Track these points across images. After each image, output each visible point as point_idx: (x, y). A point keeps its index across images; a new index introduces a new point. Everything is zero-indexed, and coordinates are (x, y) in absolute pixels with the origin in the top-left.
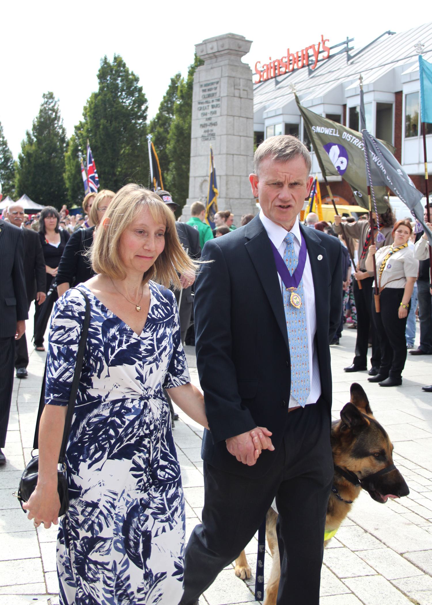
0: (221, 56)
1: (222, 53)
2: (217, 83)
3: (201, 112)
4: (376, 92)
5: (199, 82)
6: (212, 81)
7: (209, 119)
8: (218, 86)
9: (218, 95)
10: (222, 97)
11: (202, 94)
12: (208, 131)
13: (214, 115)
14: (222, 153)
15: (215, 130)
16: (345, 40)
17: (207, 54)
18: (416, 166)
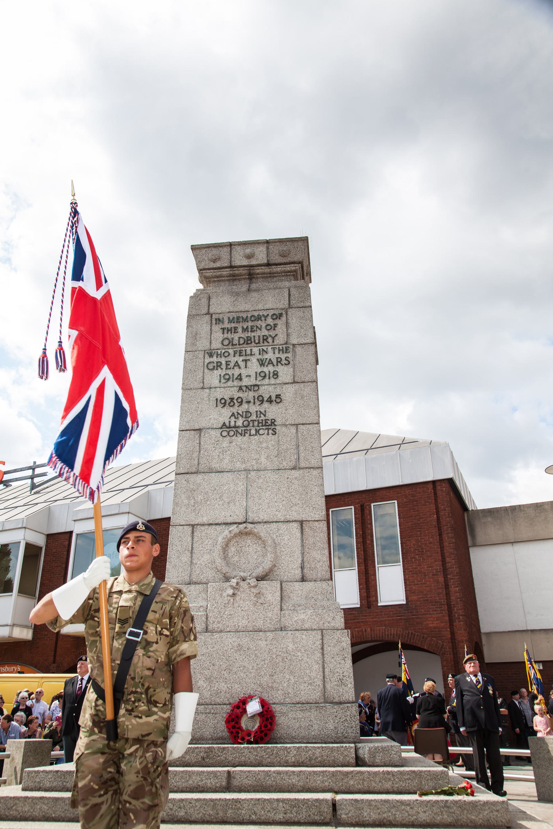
0: (271, 275)
1: (279, 269)
4: (130, 514)
5: (208, 313)
6: (256, 314)
7: (249, 388)
8: (281, 323)
9: (281, 339)
10: (294, 345)
11: (218, 336)
13: (273, 381)
14: (302, 465)
15: (272, 411)
16: (32, 464)
17: (231, 267)
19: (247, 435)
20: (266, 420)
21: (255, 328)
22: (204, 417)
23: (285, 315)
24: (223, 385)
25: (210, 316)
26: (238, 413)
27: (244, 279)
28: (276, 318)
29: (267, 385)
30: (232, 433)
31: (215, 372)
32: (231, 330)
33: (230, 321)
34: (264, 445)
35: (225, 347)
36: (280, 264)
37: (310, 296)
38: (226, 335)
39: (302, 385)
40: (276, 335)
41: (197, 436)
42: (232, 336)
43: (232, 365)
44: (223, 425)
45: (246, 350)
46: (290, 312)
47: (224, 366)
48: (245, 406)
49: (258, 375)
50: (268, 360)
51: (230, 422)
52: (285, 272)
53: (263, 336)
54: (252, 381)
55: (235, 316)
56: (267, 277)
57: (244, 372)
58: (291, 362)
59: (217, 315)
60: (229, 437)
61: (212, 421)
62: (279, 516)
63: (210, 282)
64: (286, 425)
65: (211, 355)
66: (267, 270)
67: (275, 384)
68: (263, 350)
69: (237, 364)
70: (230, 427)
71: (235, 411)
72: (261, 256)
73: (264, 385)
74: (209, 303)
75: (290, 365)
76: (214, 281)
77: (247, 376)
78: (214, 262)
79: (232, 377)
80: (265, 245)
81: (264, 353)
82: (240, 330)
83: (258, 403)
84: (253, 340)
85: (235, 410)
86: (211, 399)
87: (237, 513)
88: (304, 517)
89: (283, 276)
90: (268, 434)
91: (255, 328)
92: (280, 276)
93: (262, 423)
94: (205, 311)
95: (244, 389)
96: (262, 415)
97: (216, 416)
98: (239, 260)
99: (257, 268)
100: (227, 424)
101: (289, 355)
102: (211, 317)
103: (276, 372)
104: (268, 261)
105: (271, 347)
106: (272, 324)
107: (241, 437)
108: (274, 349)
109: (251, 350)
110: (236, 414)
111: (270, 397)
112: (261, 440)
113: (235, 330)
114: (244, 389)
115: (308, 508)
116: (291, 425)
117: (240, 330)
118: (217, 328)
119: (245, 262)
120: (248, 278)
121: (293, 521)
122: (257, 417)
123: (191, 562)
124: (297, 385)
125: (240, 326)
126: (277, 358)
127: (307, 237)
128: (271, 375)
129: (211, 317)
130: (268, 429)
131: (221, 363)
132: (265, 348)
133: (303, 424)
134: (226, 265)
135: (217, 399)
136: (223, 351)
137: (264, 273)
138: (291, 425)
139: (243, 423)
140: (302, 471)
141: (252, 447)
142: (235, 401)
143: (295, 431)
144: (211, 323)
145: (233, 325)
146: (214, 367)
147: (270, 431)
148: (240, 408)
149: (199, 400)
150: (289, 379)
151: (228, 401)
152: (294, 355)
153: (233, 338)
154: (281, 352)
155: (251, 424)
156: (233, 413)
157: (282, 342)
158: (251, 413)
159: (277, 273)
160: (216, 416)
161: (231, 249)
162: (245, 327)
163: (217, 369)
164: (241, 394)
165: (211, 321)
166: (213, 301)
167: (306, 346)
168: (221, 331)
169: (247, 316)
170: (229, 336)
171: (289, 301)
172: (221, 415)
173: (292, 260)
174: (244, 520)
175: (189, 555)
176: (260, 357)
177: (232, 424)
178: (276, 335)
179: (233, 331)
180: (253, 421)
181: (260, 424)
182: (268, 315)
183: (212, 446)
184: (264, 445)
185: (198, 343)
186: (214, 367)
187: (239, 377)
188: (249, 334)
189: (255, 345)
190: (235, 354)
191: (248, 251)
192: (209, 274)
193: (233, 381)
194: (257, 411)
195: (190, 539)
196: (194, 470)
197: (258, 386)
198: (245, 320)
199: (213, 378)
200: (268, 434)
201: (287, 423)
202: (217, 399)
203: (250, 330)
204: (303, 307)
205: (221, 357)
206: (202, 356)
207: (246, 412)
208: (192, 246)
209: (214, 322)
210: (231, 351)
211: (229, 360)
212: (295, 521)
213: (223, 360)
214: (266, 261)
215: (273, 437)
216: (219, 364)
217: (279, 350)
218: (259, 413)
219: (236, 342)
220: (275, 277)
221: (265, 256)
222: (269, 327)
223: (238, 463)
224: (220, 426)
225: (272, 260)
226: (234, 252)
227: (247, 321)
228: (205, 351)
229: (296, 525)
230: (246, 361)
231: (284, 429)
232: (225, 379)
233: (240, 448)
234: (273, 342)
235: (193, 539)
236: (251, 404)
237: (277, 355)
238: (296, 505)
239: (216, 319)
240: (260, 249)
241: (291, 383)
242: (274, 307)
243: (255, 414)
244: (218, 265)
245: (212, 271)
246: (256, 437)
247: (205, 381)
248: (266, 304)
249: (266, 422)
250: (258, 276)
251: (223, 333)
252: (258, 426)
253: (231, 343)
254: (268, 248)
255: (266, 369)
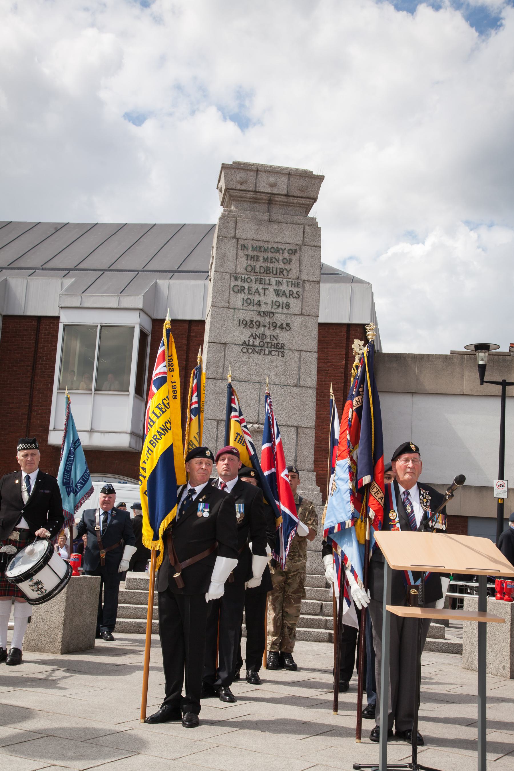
0: (288, 204)
1: (296, 200)
2: (295, 252)
3: (241, 296)
5: (234, 237)
6: (275, 246)
8: (295, 258)
9: (294, 274)
10: (304, 281)
11: (243, 262)
12: (263, 336)
13: (285, 311)
14: (302, 383)
15: (283, 337)
17: (255, 191)
18: (87, 434)
19: (262, 354)
20: (277, 343)
21: (274, 260)
22: (229, 333)
23: (298, 252)
24: (245, 308)
25: (236, 240)
26: (256, 335)
27: (264, 203)
28: (291, 254)
29: (280, 313)
30: (250, 351)
31: (239, 295)
32: (254, 258)
33: (254, 250)
34: (274, 364)
35: (248, 273)
36: (297, 197)
37: (320, 237)
38: (249, 262)
39: (307, 318)
40: (291, 269)
41: (222, 349)
42: (255, 264)
43: (253, 290)
44: (244, 343)
45: (265, 279)
46: (304, 249)
47: (246, 291)
48: (262, 329)
49: (274, 303)
50: (283, 291)
51: (249, 341)
52: (300, 204)
53: (280, 268)
54: (268, 308)
55: (258, 245)
56: (283, 205)
57: (262, 298)
58: (301, 296)
59: (243, 241)
60: (248, 354)
61: (235, 338)
62: (282, 421)
63: (233, 200)
64: (292, 350)
65: (236, 279)
66: (285, 199)
67: (286, 314)
68: (279, 281)
69: (257, 291)
70: (249, 345)
71: (254, 332)
72: (282, 187)
73: (278, 313)
74: (236, 227)
75: (300, 299)
76: (238, 200)
77: (265, 303)
78: (241, 184)
79: (252, 301)
80: (287, 176)
81: (280, 284)
82: (261, 259)
83: (272, 328)
84: (271, 271)
85: (254, 331)
86: (235, 318)
87: (251, 415)
88: (299, 424)
89: (297, 207)
90: (278, 356)
91: (274, 260)
92: (295, 206)
93: (274, 345)
94: (232, 235)
95: (262, 314)
96: (274, 339)
97: (238, 335)
98: (263, 187)
99: (277, 196)
100: (247, 343)
101: (300, 290)
102: (238, 241)
103: (288, 304)
104: (288, 192)
105: (285, 280)
106: (288, 258)
107: (257, 355)
108: (288, 282)
109: (269, 280)
110: (254, 335)
111: (282, 324)
112: (273, 359)
113: (257, 258)
114: (262, 314)
115: (303, 418)
116: (297, 350)
117: (261, 259)
118: (241, 253)
119: (268, 190)
120: (268, 203)
121: (291, 426)
122: (270, 340)
123: (216, 447)
124: (303, 317)
125: (261, 255)
126: (290, 291)
127: (324, 176)
128: (284, 305)
129: (238, 241)
130: (279, 352)
131: (244, 287)
132: (280, 280)
133: (305, 351)
134: (251, 189)
135: (240, 320)
136: (247, 277)
137: (282, 202)
138: (297, 350)
139: (259, 344)
140: (301, 389)
141: (265, 364)
142: (254, 324)
143: (298, 356)
144: (237, 248)
145: (256, 253)
146: (238, 290)
147: (280, 354)
148: (258, 330)
149: (225, 318)
150: (297, 311)
151: (249, 323)
152: (303, 291)
153: (255, 266)
154: (293, 286)
155: (266, 346)
156: (252, 334)
157: (295, 277)
158: (266, 336)
159: (293, 203)
160: (238, 335)
161: (257, 174)
162: (266, 257)
163: (241, 293)
164: (259, 318)
165: (237, 245)
166: (239, 225)
167: (313, 283)
168: (245, 257)
169: (268, 247)
170: (252, 263)
171: (303, 238)
172: (242, 334)
173: (308, 196)
174: (257, 421)
175: (215, 442)
176: (276, 287)
177: (251, 343)
178: (291, 269)
179: (255, 259)
180: (267, 343)
181: (273, 347)
182: (285, 249)
183: (234, 359)
184: (274, 364)
185: (225, 265)
186: (238, 290)
187: (258, 303)
188: (269, 265)
189: (273, 275)
190: (256, 281)
191: (272, 180)
192: (235, 193)
193: (253, 306)
194: (271, 335)
195: (215, 430)
196: (219, 376)
197: (273, 313)
198: (266, 250)
199: (238, 300)
200: (278, 356)
201: (293, 349)
202: (240, 320)
203: (269, 261)
204: (314, 246)
205: (244, 282)
206: (229, 278)
207: (262, 334)
208: (223, 164)
209: (240, 247)
210: (253, 278)
211: (251, 286)
212: (293, 426)
213: (246, 285)
214: (286, 193)
215: (282, 358)
216: (243, 288)
217: (292, 284)
218: (272, 336)
219: (257, 270)
220: (291, 206)
221: (285, 187)
222: (285, 261)
223: (254, 376)
224: (241, 343)
225: (291, 191)
226: (259, 178)
227: (268, 252)
228: (231, 273)
229: (293, 429)
230: (265, 289)
231: (290, 353)
232: (247, 302)
233: (256, 364)
234: (288, 275)
235: (217, 430)
236: (267, 328)
237: (290, 288)
238: (294, 414)
239: (242, 245)
240: (282, 180)
241: (299, 315)
242: (291, 242)
243: (269, 337)
244: (244, 187)
245: (238, 192)
246: (268, 356)
247: (230, 301)
248: (284, 237)
249: (277, 346)
250: (276, 203)
251: (247, 260)
252: (271, 348)
253: (253, 269)
254: (289, 180)
255: (280, 299)
